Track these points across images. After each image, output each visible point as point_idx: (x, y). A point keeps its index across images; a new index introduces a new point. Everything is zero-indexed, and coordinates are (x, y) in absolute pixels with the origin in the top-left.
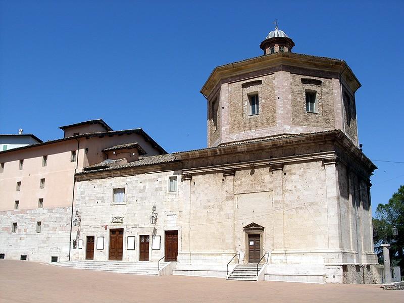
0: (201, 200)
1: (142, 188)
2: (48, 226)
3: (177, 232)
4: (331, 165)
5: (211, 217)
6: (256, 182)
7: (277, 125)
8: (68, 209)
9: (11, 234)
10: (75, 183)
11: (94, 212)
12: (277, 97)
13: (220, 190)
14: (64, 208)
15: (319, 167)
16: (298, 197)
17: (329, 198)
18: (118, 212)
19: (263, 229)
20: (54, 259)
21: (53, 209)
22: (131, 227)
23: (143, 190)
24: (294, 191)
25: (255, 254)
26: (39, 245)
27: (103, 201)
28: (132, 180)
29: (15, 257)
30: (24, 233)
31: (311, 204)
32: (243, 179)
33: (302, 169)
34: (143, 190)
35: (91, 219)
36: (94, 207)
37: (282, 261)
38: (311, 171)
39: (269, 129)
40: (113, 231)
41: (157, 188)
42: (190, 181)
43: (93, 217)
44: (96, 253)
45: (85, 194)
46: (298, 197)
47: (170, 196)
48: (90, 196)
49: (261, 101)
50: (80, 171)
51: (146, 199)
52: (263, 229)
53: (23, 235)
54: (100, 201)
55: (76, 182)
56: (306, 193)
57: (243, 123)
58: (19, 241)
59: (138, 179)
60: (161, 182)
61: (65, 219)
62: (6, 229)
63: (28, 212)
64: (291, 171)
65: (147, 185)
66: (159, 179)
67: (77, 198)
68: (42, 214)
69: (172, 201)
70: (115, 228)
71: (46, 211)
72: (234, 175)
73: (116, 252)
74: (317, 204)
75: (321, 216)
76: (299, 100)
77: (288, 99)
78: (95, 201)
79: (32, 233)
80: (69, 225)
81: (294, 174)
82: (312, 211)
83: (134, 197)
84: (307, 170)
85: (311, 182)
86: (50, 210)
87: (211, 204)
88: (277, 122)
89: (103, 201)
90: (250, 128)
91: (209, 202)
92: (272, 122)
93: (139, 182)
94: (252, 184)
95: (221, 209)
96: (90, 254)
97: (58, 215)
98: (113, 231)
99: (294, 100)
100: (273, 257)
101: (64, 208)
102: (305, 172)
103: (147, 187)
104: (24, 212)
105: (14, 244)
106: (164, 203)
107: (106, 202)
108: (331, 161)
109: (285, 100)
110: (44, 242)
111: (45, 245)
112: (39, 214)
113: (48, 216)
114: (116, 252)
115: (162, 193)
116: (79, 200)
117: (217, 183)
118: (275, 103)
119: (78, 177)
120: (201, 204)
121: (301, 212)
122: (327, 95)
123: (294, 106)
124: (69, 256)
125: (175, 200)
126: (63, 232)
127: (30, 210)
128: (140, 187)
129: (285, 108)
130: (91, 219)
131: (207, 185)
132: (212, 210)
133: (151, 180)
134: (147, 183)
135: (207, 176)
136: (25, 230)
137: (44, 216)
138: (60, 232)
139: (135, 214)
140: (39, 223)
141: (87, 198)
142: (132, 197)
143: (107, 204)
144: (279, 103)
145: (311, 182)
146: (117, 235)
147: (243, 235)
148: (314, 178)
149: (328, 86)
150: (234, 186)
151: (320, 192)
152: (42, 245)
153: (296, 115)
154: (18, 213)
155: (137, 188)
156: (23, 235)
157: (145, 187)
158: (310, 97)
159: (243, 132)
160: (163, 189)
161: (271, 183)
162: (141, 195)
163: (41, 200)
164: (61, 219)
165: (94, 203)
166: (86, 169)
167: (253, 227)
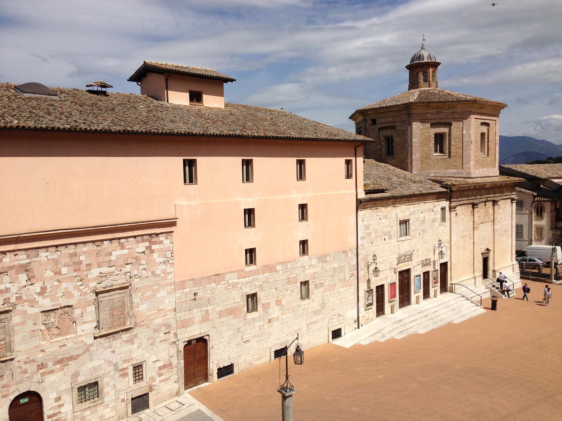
2: (322, 285)
8: (350, 253)
9: (245, 319)
14: (344, 252)
20: (337, 334)
26: (310, 321)
29: (259, 359)
30: (277, 308)
34: (423, 222)
36: (382, 246)
41: (433, 219)
45: (371, 229)
48: (376, 231)
53: (275, 312)
54: (387, 237)
55: (359, 212)
56: (505, 223)
58: (266, 326)
61: (347, 269)
62: (231, 312)
63: (279, 268)
65: (426, 215)
68: (308, 267)
71: (314, 262)
78: (382, 238)
79: (293, 304)
80: (353, 277)
86: (322, 259)
87: (465, 233)
97: (336, 265)
101: (344, 252)
103: (426, 218)
104: (271, 268)
105: (255, 337)
107: (393, 237)
110: (316, 313)
111: (320, 317)
112: (304, 267)
113: (319, 269)
116: (363, 238)
119: (360, 204)
126: (345, 289)
127: (282, 263)
131: (463, 216)
135: (463, 207)
136: (278, 303)
137: (312, 271)
138: (341, 290)
140: (305, 283)
141: (373, 235)
146: (405, 275)
152: (315, 318)
154: (257, 272)
156: (275, 312)
157: (424, 217)
160: (438, 220)
163: (304, 243)
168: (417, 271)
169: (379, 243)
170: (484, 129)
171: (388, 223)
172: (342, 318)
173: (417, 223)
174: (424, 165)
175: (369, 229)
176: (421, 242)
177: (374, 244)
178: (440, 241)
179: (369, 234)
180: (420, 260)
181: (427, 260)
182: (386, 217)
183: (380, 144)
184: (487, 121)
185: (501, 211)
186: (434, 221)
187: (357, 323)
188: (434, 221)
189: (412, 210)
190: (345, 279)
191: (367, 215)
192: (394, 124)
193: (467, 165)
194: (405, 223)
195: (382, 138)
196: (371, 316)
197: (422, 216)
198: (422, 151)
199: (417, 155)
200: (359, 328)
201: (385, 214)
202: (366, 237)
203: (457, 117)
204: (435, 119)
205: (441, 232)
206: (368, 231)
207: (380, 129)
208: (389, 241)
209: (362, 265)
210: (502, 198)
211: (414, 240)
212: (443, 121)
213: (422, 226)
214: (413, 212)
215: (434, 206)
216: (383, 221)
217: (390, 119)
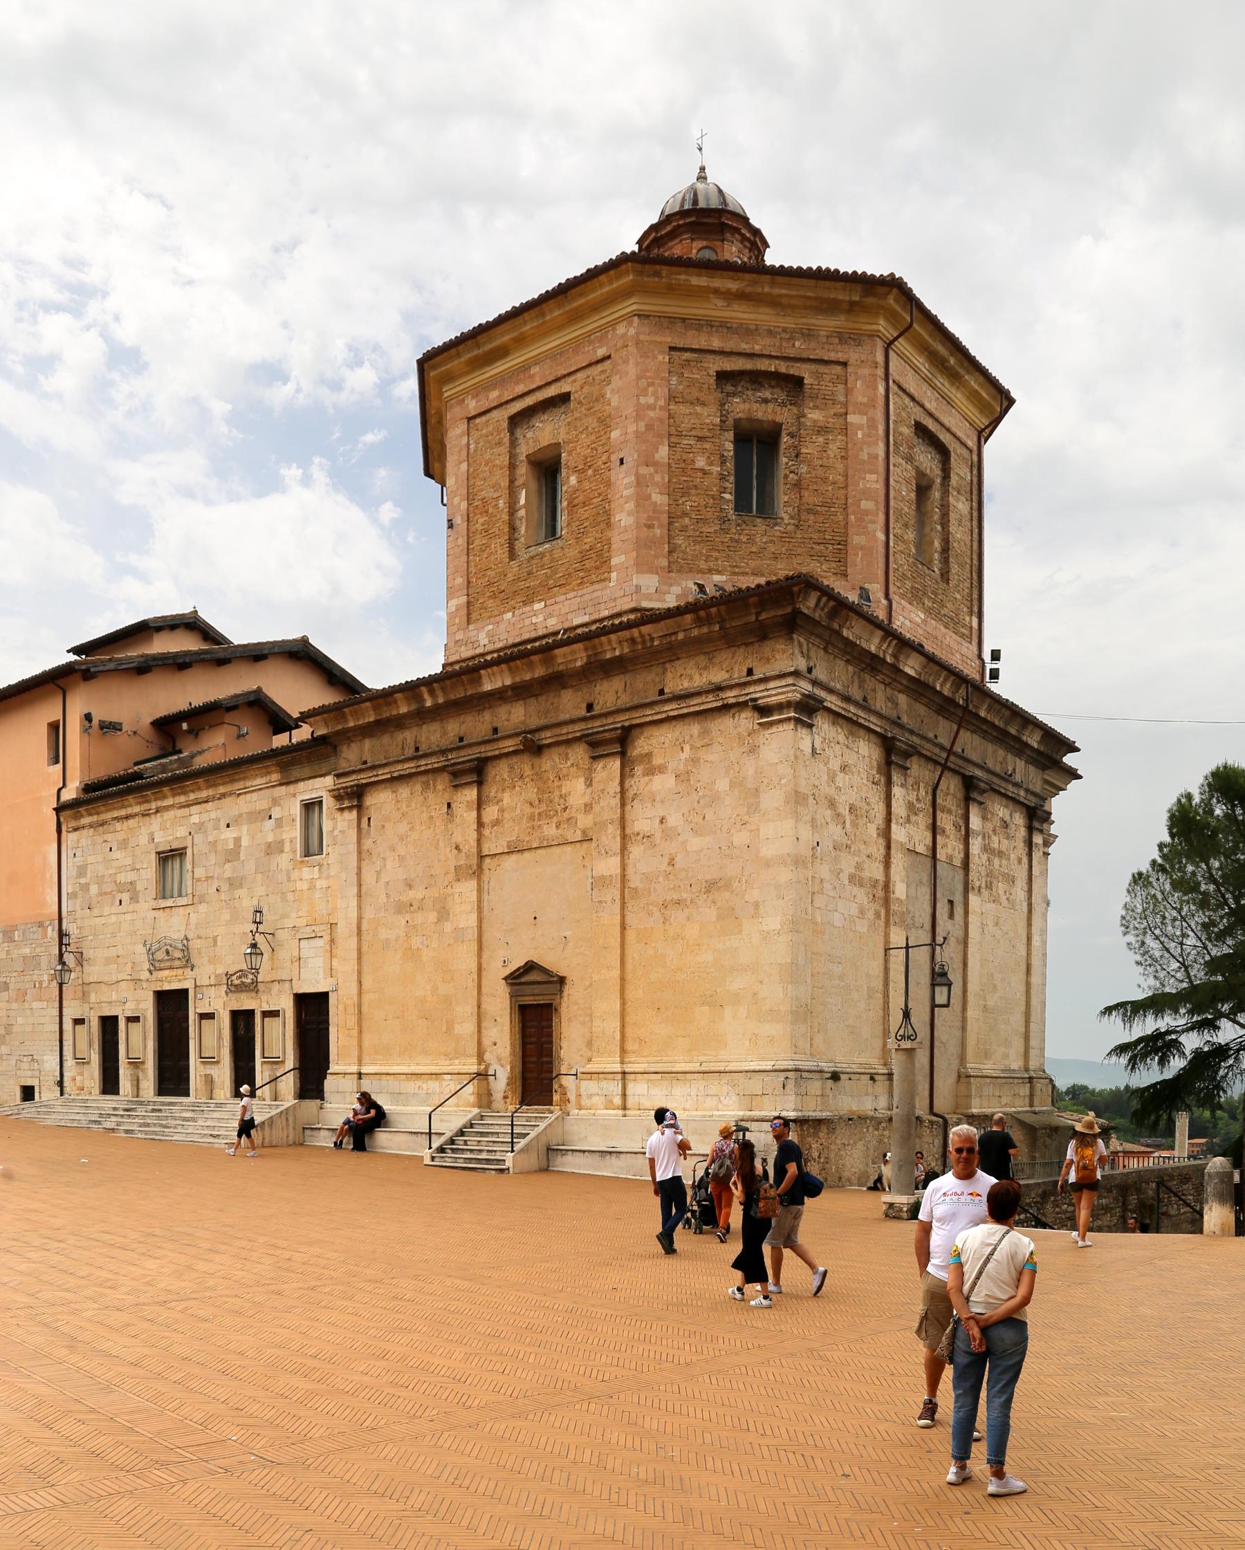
0: (387, 883)
3: (325, 996)
4: (781, 728)
5: (416, 942)
6: (543, 807)
7: (614, 575)
11: (114, 935)
12: (615, 458)
13: (441, 845)
15: (740, 737)
16: (671, 863)
17: (767, 864)
18: (174, 926)
19: (562, 980)
21: (14, 928)
23: (232, 855)
24: (658, 835)
25: (537, 1078)
28: (205, 817)
31: (711, 886)
32: (507, 798)
33: (687, 748)
34: (232, 855)
35: (108, 961)
36: (113, 919)
37: (611, 1102)
38: (713, 755)
39: (590, 593)
41: (269, 845)
42: (355, 813)
43: (113, 952)
45: (89, 875)
46: (671, 863)
47: (306, 873)
48: (100, 880)
49: (569, 481)
50: (69, 794)
51: (241, 886)
52: (562, 980)
55: (70, 839)
56: (695, 843)
57: (510, 577)
59: (219, 813)
60: (279, 822)
61: (44, 962)
64: (650, 762)
65: (244, 831)
66: (276, 813)
69: (312, 887)
72: (480, 783)
74: (728, 886)
75: (740, 932)
76: (701, 462)
77: (655, 464)
78: (114, 897)
81: (661, 769)
82: (712, 913)
84: (703, 754)
85: (715, 799)
87: (416, 894)
88: (614, 561)
90: (528, 601)
91: (410, 887)
92: (596, 563)
94: (532, 817)
97: (27, 951)
99: (680, 470)
100: (589, 1086)
101: (41, 925)
102: (695, 761)
103: (245, 842)
106: (290, 896)
107: (141, 899)
108: (780, 707)
109: (644, 470)
115: (283, 860)
116: (72, 896)
117: (431, 817)
118: (608, 484)
120: (388, 896)
121: (678, 916)
122: (821, 439)
123: (677, 491)
124: (61, 1084)
125: (321, 884)
128: (226, 840)
129: (642, 499)
130: (108, 961)
131: (403, 828)
132: (419, 918)
134: (245, 828)
135: (404, 791)
138: (35, 1005)
139: (215, 939)
141: (94, 889)
142: (207, 878)
144: (623, 481)
145: (715, 799)
147: (499, 1003)
148: (723, 785)
149: (826, 400)
150: (480, 824)
151: (741, 838)
153: (684, 529)
155: (219, 847)
157: (237, 840)
158: (757, 448)
159: (509, 615)
160: (287, 847)
161: (588, 807)
162: (228, 870)
165: (113, 904)
166: (88, 788)
168: (212, 1002)
169: (107, 911)
171: (129, 861)
176: (226, 916)
177: (96, 912)
180: (221, 970)
182: (123, 845)
185: (662, 783)
186: (273, 849)
188: (273, 849)
189: (195, 819)
190: (41, 983)
191: (83, 842)
194: (169, 857)
197: (229, 834)
201: (121, 836)
202: (80, 894)
205: (305, 886)
206: (83, 881)
210: (649, 714)
211: (202, 908)
213: (228, 866)
214: (201, 826)
215: (275, 802)
216: (116, 854)
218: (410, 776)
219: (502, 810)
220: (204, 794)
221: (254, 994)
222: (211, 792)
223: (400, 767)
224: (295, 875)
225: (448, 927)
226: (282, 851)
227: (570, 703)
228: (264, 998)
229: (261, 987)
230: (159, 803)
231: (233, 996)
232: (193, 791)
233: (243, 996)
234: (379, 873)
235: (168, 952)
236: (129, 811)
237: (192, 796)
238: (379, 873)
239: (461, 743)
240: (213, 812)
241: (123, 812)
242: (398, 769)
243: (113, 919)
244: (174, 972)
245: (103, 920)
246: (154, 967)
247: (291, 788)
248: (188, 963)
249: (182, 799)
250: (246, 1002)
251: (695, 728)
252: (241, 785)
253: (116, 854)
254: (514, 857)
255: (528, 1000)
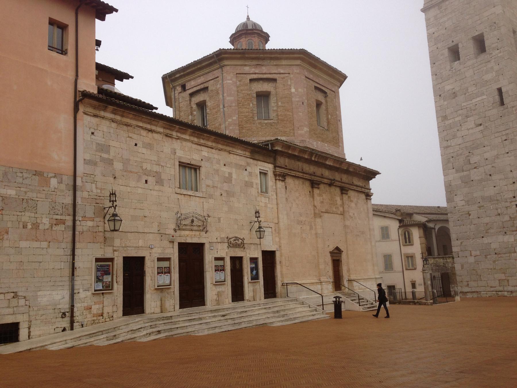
0: (294, 212)
1: (227, 175)
8: (54, 182)
10: (76, 110)
18: (192, 206)
22: (216, 241)
27: (160, 182)
34: (228, 179)
36: (140, 191)
40: (183, 248)
41: (246, 182)
44: (151, 301)
54: (150, 179)
66: (249, 169)
67: (88, 157)
70: (189, 241)
73: (192, 293)
78: (140, 177)
83: (217, 187)
87: (302, 219)
89: (160, 182)
93: (222, 164)
95: (311, 228)
96: (133, 303)
97: (11, 192)
98: (183, 248)
103: (234, 176)
114: (192, 293)
125: (269, 205)
126: (36, 244)
131: (297, 194)
133: (238, 166)
138: (23, 244)
139: (219, 219)
141: (118, 166)
143: (169, 190)
148: (362, 209)
157: (230, 174)
160: (255, 186)
162: (226, 186)
164: (27, 204)
165: (138, 180)
167: (335, 251)
170: (320, 97)
172: (22, 302)
173: (217, 178)
174: (244, 131)
175: (108, 152)
176: (225, 209)
178: (257, 212)
179: (110, 162)
180: (223, 235)
181: (237, 238)
182: (149, 146)
183: (192, 114)
184: (326, 90)
185: (353, 205)
186: (248, 185)
187: (67, 319)
188: (248, 185)
190: (36, 226)
192: (206, 85)
193: (300, 132)
194: (190, 168)
195: (194, 106)
196: (108, 310)
197: (226, 170)
198: (242, 113)
199: (235, 118)
200: (72, 328)
201: (147, 140)
203: (282, 71)
204: (255, 74)
207: (192, 95)
208: (157, 187)
209: (85, 209)
211: (211, 201)
212: (265, 76)
213: (225, 184)
214: (208, 159)
215: (248, 164)
217: (202, 80)
218: (298, 177)
219: (323, 199)
220: (210, 144)
221: (242, 249)
222: (214, 144)
223: (298, 173)
224: (259, 199)
225: (313, 232)
226: (253, 187)
227: (337, 176)
228: (248, 251)
229: (246, 246)
230: (179, 135)
231: (231, 249)
232: (203, 139)
233: (237, 250)
234: (291, 208)
235: (193, 221)
236: (154, 128)
237: (202, 141)
238: (291, 208)
239: (314, 174)
240: (215, 155)
241: (149, 126)
242: (298, 174)
243: (140, 191)
244: (194, 233)
245: (129, 189)
246: (179, 227)
247: (255, 162)
248: (204, 229)
249: (196, 140)
250: (238, 253)
251: (356, 194)
252: (231, 149)
253: (140, 149)
254: (327, 214)
255: (335, 258)
